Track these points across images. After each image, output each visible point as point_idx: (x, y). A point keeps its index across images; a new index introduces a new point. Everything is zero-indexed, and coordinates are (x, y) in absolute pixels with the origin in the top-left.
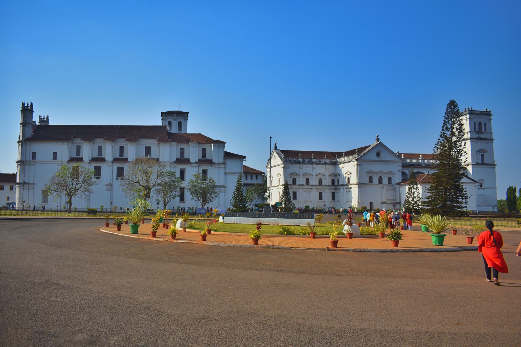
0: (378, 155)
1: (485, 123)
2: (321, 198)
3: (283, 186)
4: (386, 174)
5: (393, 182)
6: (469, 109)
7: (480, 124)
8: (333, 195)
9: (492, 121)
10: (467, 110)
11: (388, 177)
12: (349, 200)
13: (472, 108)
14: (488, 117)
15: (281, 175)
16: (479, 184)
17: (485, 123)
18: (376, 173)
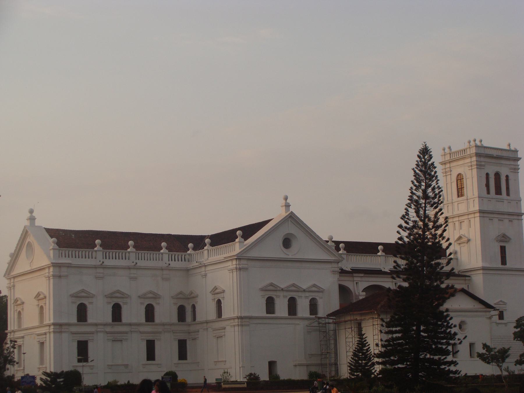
0: (287, 243)
1: (507, 177)
2: (151, 355)
3: (52, 327)
4: (304, 291)
5: (322, 312)
6: (477, 142)
7: (497, 175)
8: (182, 345)
9: (519, 171)
10: (472, 143)
11: (311, 297)
12: (220, 360)
13: (481, 141)
14: (512, 163)
15: (47, 298)
16: (497, 313)
17: (507, 177)
18: (282, 289)
